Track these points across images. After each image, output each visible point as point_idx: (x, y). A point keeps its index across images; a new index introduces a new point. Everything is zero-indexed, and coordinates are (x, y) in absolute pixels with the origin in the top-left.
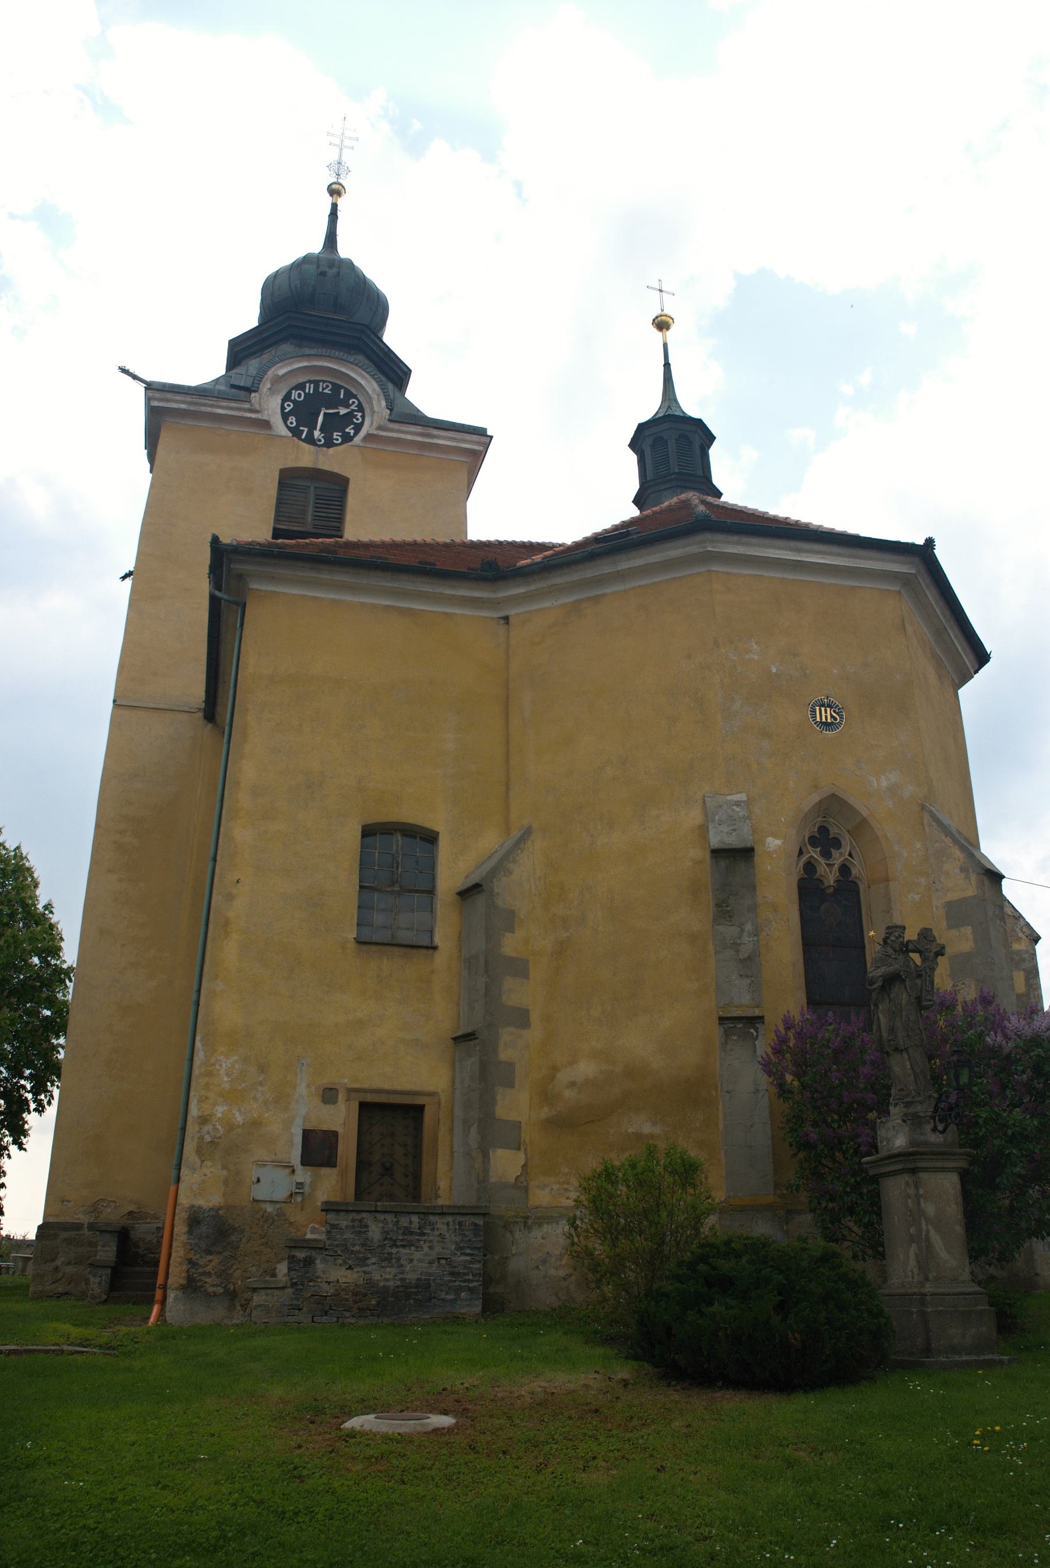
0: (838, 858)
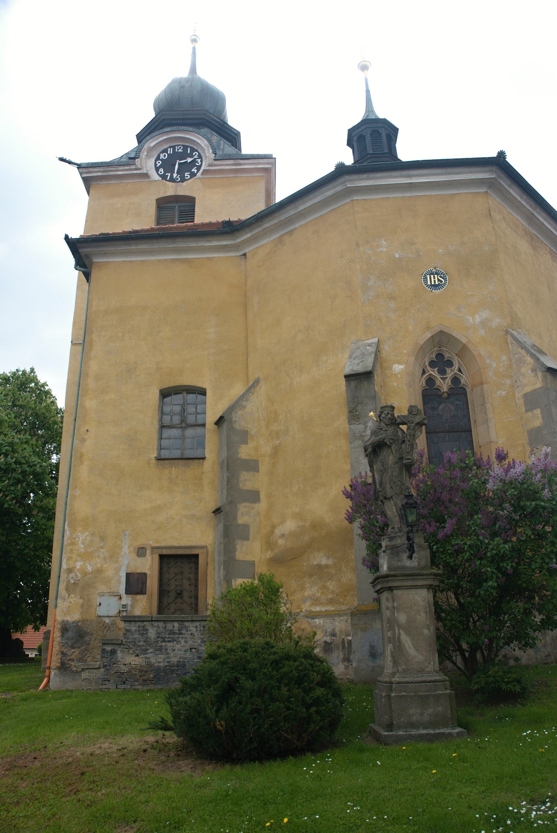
0: (450, 374)
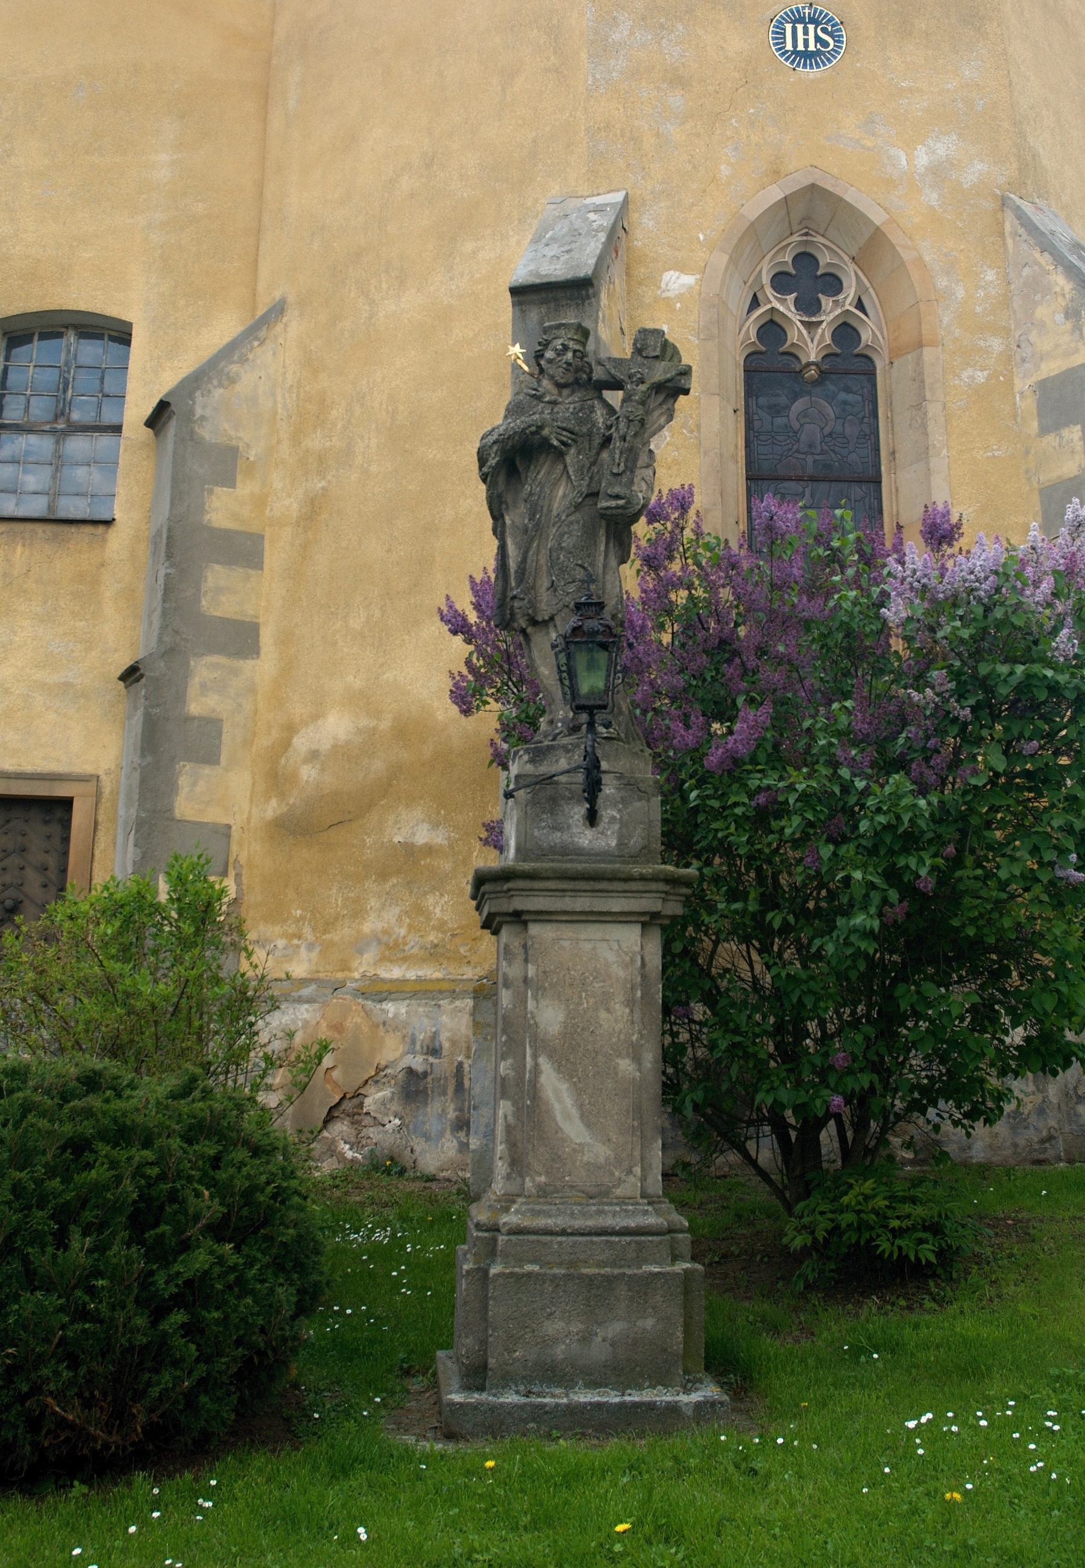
0: (830, 312)
